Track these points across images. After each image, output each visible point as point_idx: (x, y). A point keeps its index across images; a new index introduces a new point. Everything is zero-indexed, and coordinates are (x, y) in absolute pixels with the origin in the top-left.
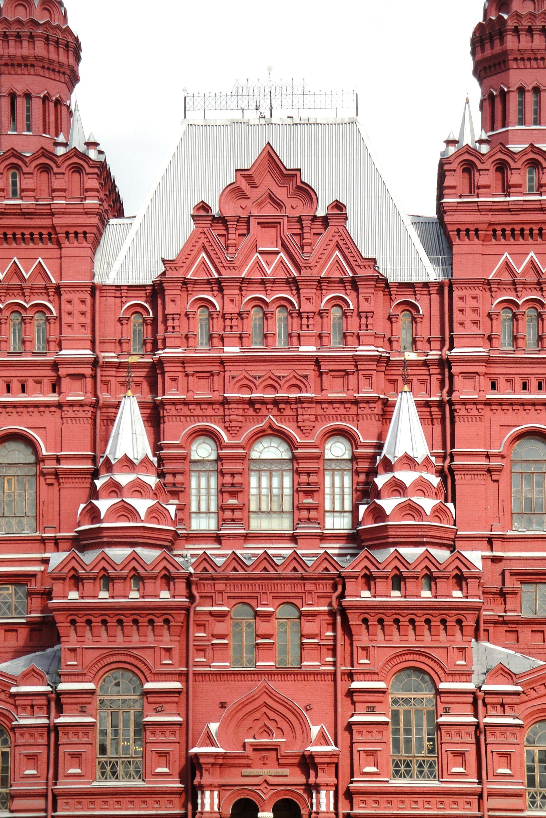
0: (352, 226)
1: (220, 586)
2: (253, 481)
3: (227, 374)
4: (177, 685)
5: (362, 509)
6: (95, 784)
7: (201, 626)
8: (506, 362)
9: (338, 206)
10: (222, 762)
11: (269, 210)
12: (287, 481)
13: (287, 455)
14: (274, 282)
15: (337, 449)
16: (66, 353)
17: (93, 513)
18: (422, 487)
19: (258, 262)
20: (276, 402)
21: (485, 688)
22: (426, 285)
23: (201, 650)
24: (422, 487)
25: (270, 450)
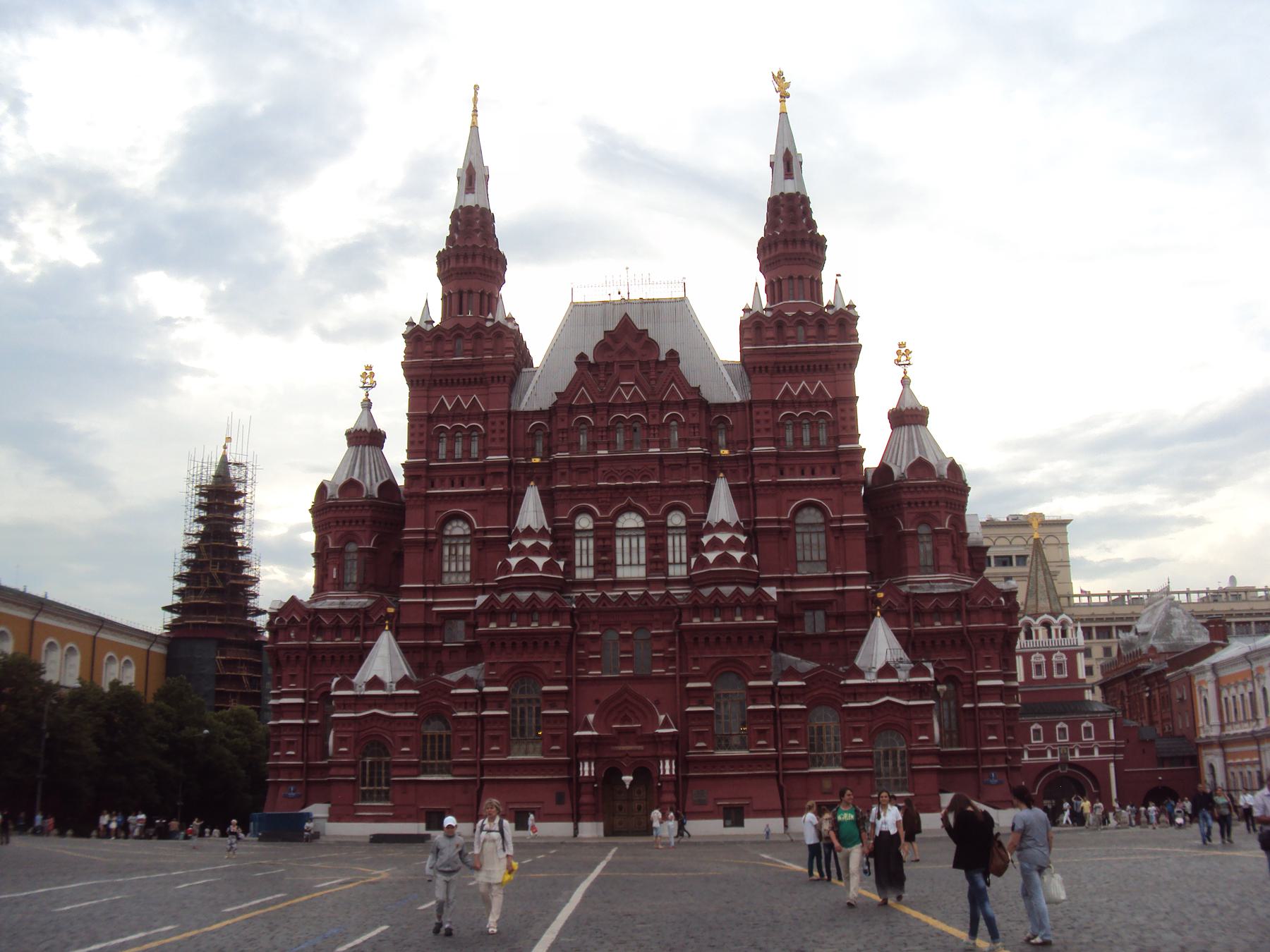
0: (683, 366)
1: (594, 617)
2: (619, 543)
3: (600, 469)
4: (565, 688)
5: (693, 560)
6: (510, 758)
7: (581, 646)
8: (789, 456)
9: (673, 355)
11: (626, 358)
12: (643, 541)
13: (642, 524)
14: (631, 405)
15: (676, 519)
17: (506, 567)
18: (734, 543)
19: (619, 392)
21: (780, 684)
22: (734, 405)
23: (582, 662)
24: (734, 543)
25: (630, 521)
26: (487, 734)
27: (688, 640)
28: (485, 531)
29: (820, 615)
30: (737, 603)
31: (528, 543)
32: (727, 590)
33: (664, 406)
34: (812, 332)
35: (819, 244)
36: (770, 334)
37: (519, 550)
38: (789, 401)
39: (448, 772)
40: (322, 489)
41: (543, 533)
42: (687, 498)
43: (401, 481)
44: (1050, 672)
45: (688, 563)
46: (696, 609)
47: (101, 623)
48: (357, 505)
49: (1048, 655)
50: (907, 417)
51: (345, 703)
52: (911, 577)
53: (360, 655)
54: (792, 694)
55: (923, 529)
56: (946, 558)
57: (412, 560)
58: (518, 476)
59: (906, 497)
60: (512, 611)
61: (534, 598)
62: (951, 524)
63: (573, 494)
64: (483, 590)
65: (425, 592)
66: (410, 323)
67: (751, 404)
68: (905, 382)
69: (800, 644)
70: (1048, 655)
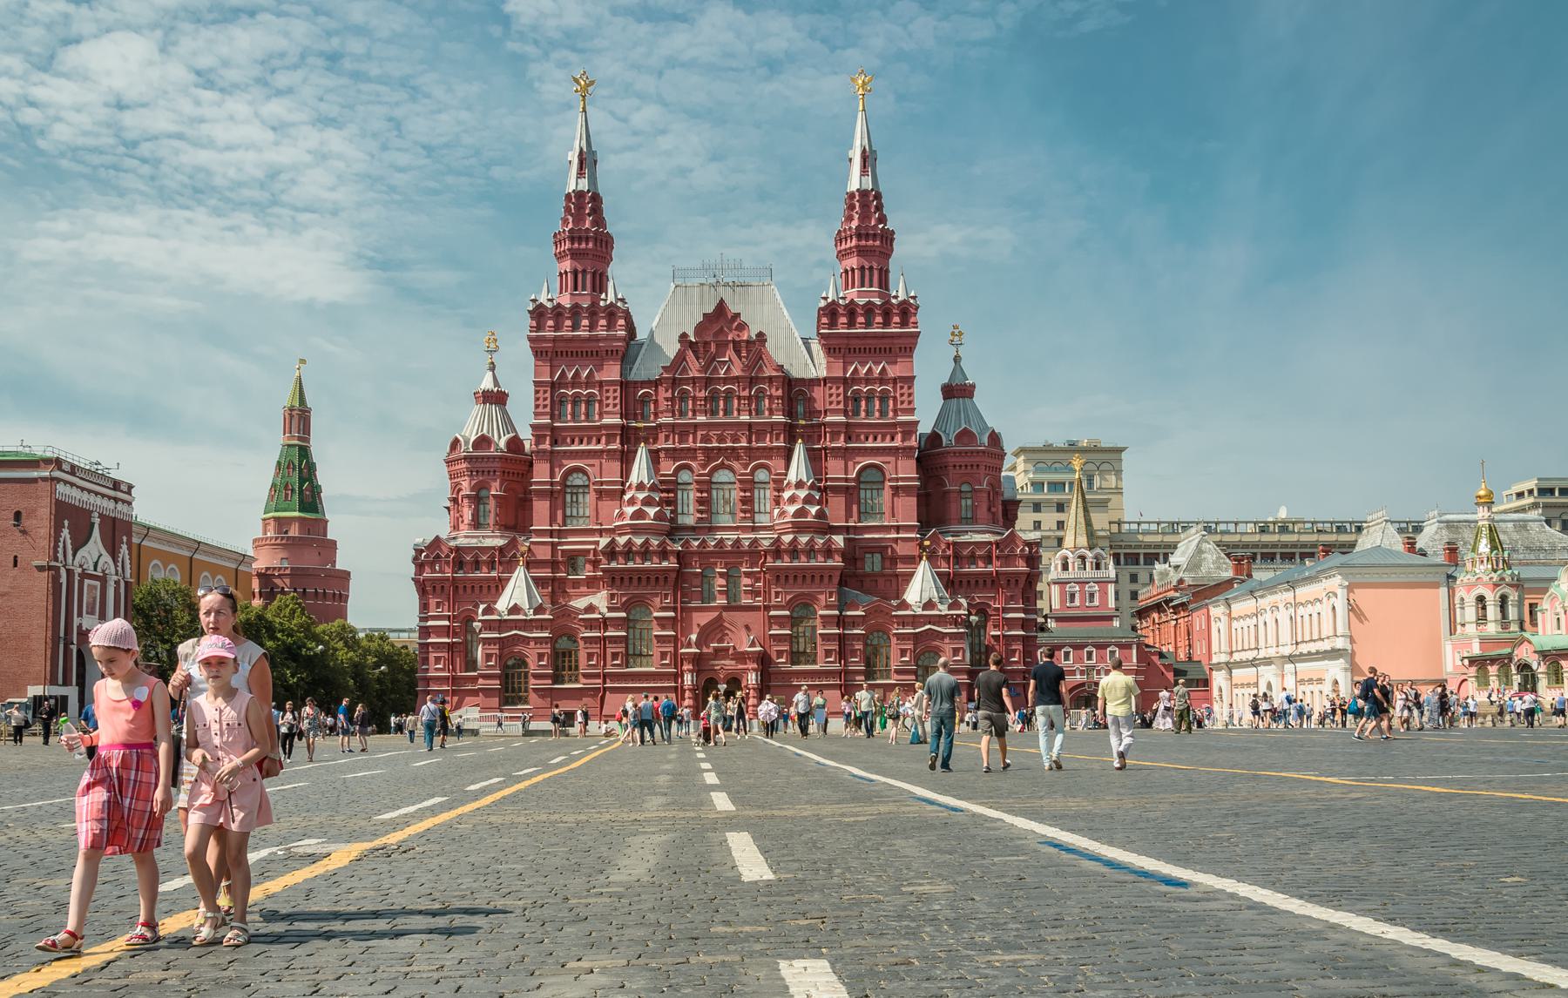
7: (684, 581)
9: (761, 335)
10: (697, 660)
15: (762, 475)
16: (606, 421)
17: (621, 515)
20: (727, 449)
25: (723, 476)
26: (609, 651)
28: (602, 483)
29: (878, 557)
30: (810, 551)
31: (641, 496)
32: (804, 539)
33: (752, 381)
34: (879, 319)
35: (888, 238)
36: (844, 320)
37: (632, 502)
38: (855, 380)
39: (577, 681)
40: (455, 444)
41: (653, 488)
42: (770, 458)
43: (526, 435)
44: (1083, 600)
45: (771, 513)
47: (198, 545)
48: (488, 458)
50: (957, 391)
51: (488, 625)
52: (954, 528)
53: (499, 585)
54: (854, 622)
55: (965, 488)
56: (983, 512)
57: (541, 508)
58: (629, 438)
59: (951, 460)
60: (628, 552)
61: (647, 542)
62: (990, 484)
63: (673, 454)
64: (601, 532)
65: (551, 533)
66: (534, 301)
67: (825, 379)
68: (957, 359)
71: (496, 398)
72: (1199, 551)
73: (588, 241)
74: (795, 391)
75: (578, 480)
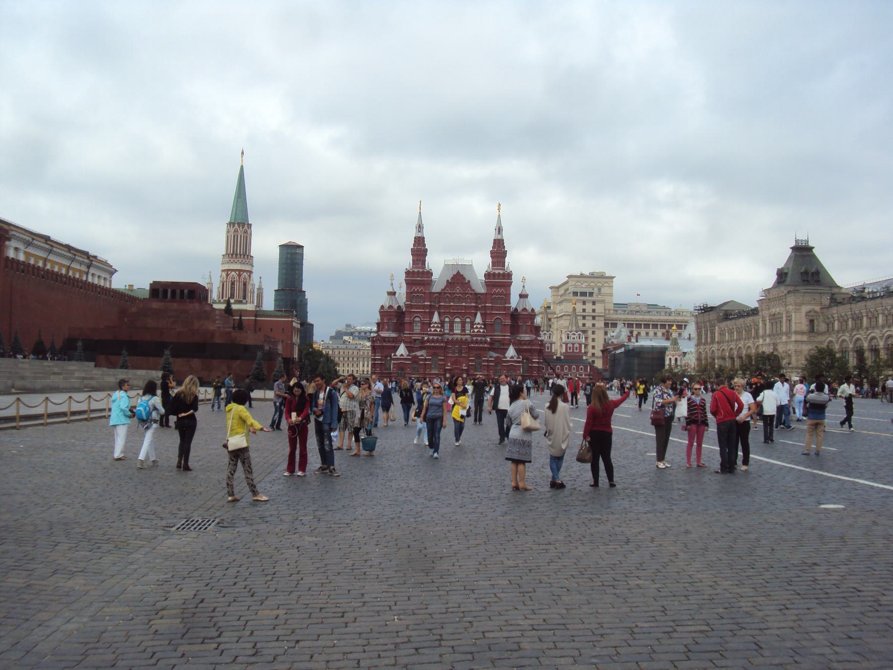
15: (468, 320)
25: (457, 320)
27: (470, 349)
30: (481, 342)
38: (495, 294)
40: (382, 307)
46: (472, 342)
49: (573, 344)
50: (523, 296)
53: (396, 349)
54: (491, 361)
57: (407, 326)
60: (433, 341)
63: (445, 313)
69: (494, 350)
70: (573, 344)
71: (392, 294)
72: (620, 331)
73: (419, 250)
74: (477, 296)
75: (417, 319)
